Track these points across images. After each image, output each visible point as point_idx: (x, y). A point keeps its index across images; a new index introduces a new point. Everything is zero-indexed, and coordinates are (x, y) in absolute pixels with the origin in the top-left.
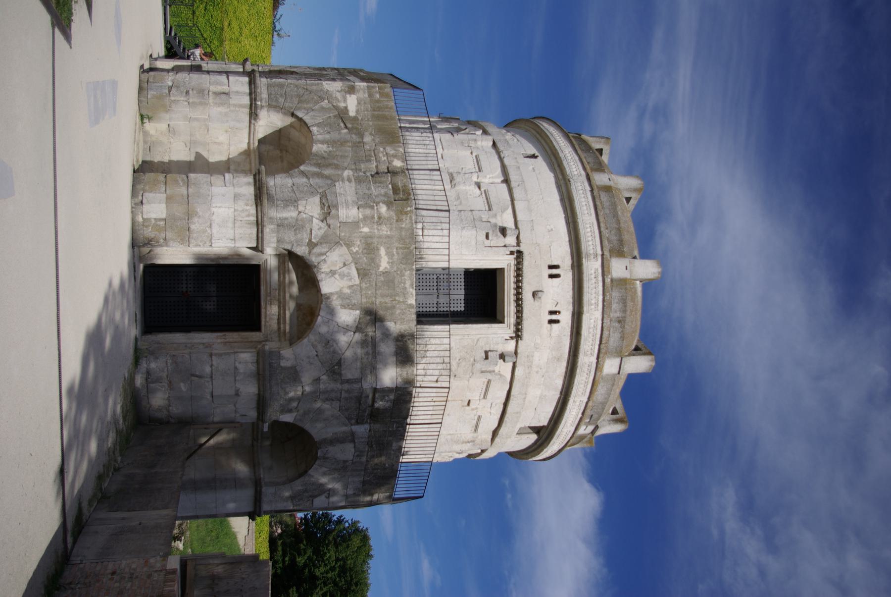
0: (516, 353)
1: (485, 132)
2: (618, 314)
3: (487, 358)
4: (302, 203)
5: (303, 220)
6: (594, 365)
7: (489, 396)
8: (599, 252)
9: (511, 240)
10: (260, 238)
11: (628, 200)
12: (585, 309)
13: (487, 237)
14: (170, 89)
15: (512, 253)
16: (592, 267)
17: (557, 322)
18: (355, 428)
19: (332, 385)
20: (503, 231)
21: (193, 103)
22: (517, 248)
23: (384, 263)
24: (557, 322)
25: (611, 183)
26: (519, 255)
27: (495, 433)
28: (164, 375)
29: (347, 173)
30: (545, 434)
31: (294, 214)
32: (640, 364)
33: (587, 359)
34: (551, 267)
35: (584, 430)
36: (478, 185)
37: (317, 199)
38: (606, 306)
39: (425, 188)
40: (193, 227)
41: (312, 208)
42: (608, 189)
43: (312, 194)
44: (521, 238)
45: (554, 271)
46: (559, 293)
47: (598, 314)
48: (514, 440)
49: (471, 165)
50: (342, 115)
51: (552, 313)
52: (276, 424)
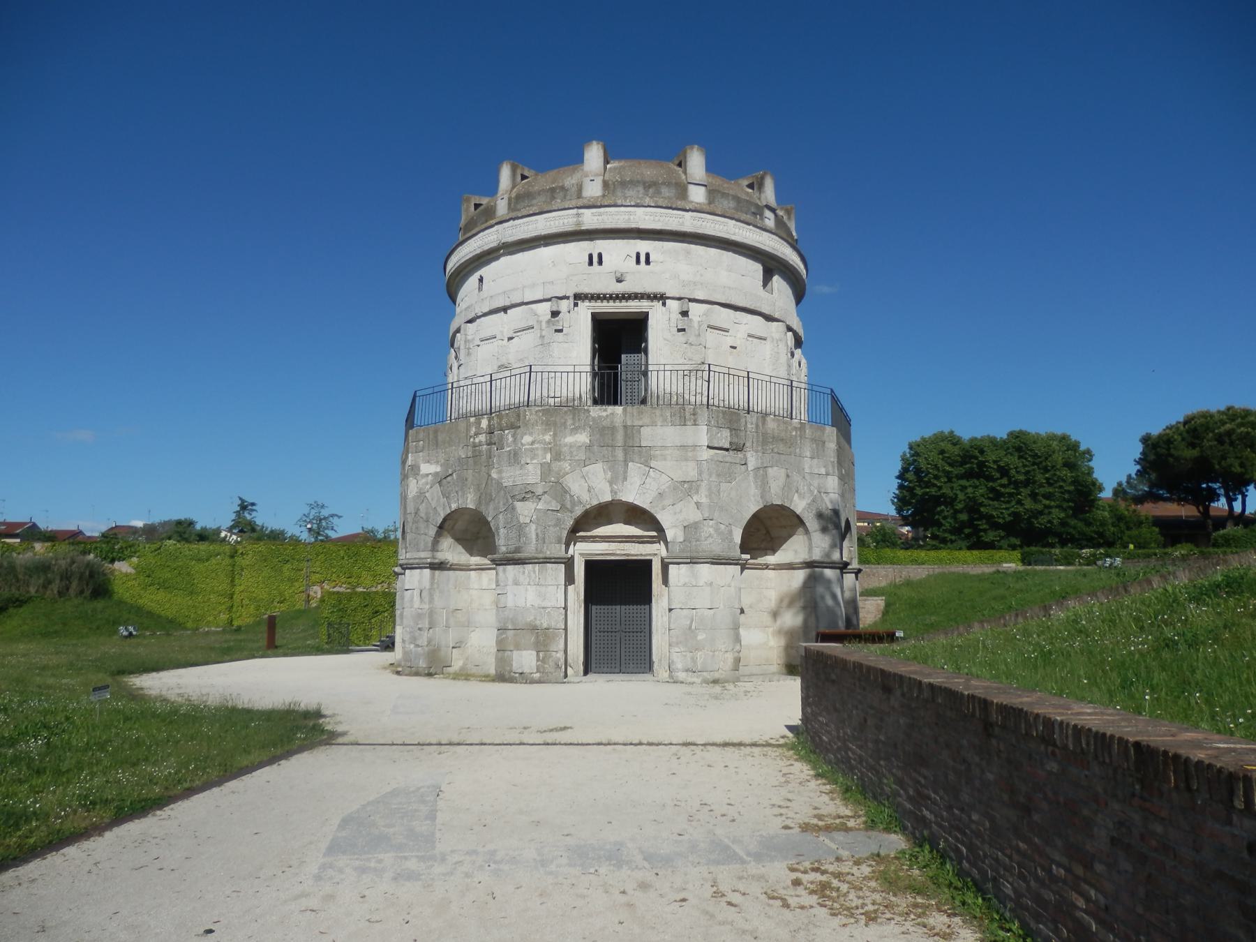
0: (679, 299)
1: (458, 331)
2: (641, 189)
3: (683, 330)
4: (522, 520)
5: (538, 519)
6: (695, 214)
7: (724, 326)
8: (575, 211)
9: (564, 306)
11: (524, 177)
12: (633, 226)
13: (557, 331)
14: (417, 646)
15: (576, 305)
16: (591, 220)
17: (648, 255)
18: (751, 466)
19: (704, 491)
20: (555, 314)
21: (430, 623)
22: (572, 299)
24: (648, 255)
25: (506, 197)
26: (579, 297)
27: (769, 318)
28: (689, 655)
29: (494, 475)
30: (772, 266)
31: (533, 527)
32: (696, 162)
34: (591, 263)
35: (770, 221)
36: (510, 339)
37: (518, 505)
39: (509, 394)
40: (545, 625)
41: (525, 510)
43: (514, 509)
44: (561, 295)
45: (595, 259)
47: (640, 211)
48: (780, 295)
49: (487, 348)
50: (441, 480)
51: (638, 262)
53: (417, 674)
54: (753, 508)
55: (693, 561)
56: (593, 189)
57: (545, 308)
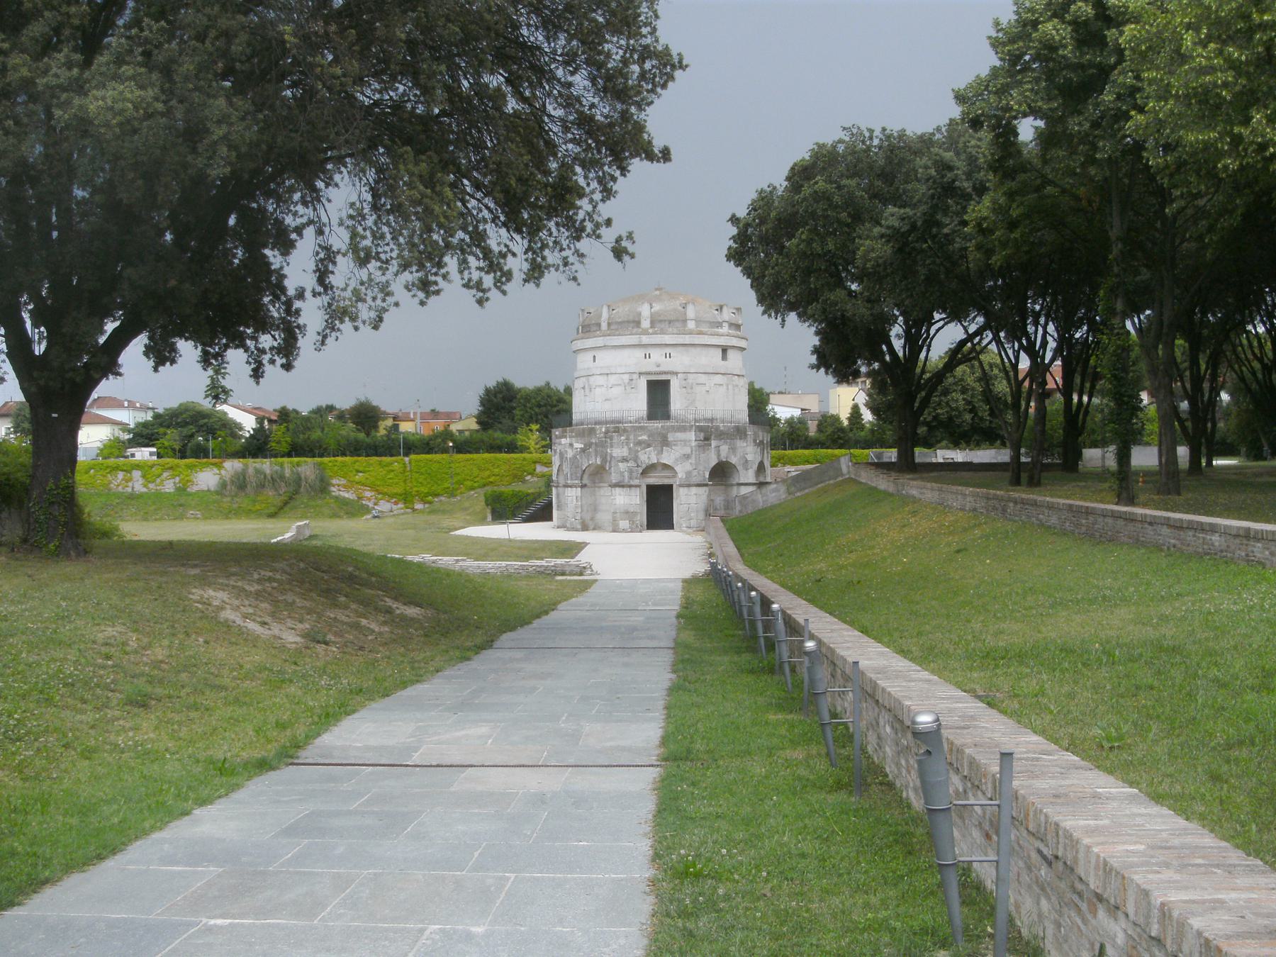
9: (635, 376)
10: (636, 486)
16: (645, 339)
23: (645, 437)
33: (687, 339)
38: (663, 332)
42: (609, 324)
46: (657, 355)
50: (583, 450)
52: (710, 479)
53: (577, 530)
54: (714, 462)
55: (689, 486)
56: (646, 324)
57: (626, 377)
